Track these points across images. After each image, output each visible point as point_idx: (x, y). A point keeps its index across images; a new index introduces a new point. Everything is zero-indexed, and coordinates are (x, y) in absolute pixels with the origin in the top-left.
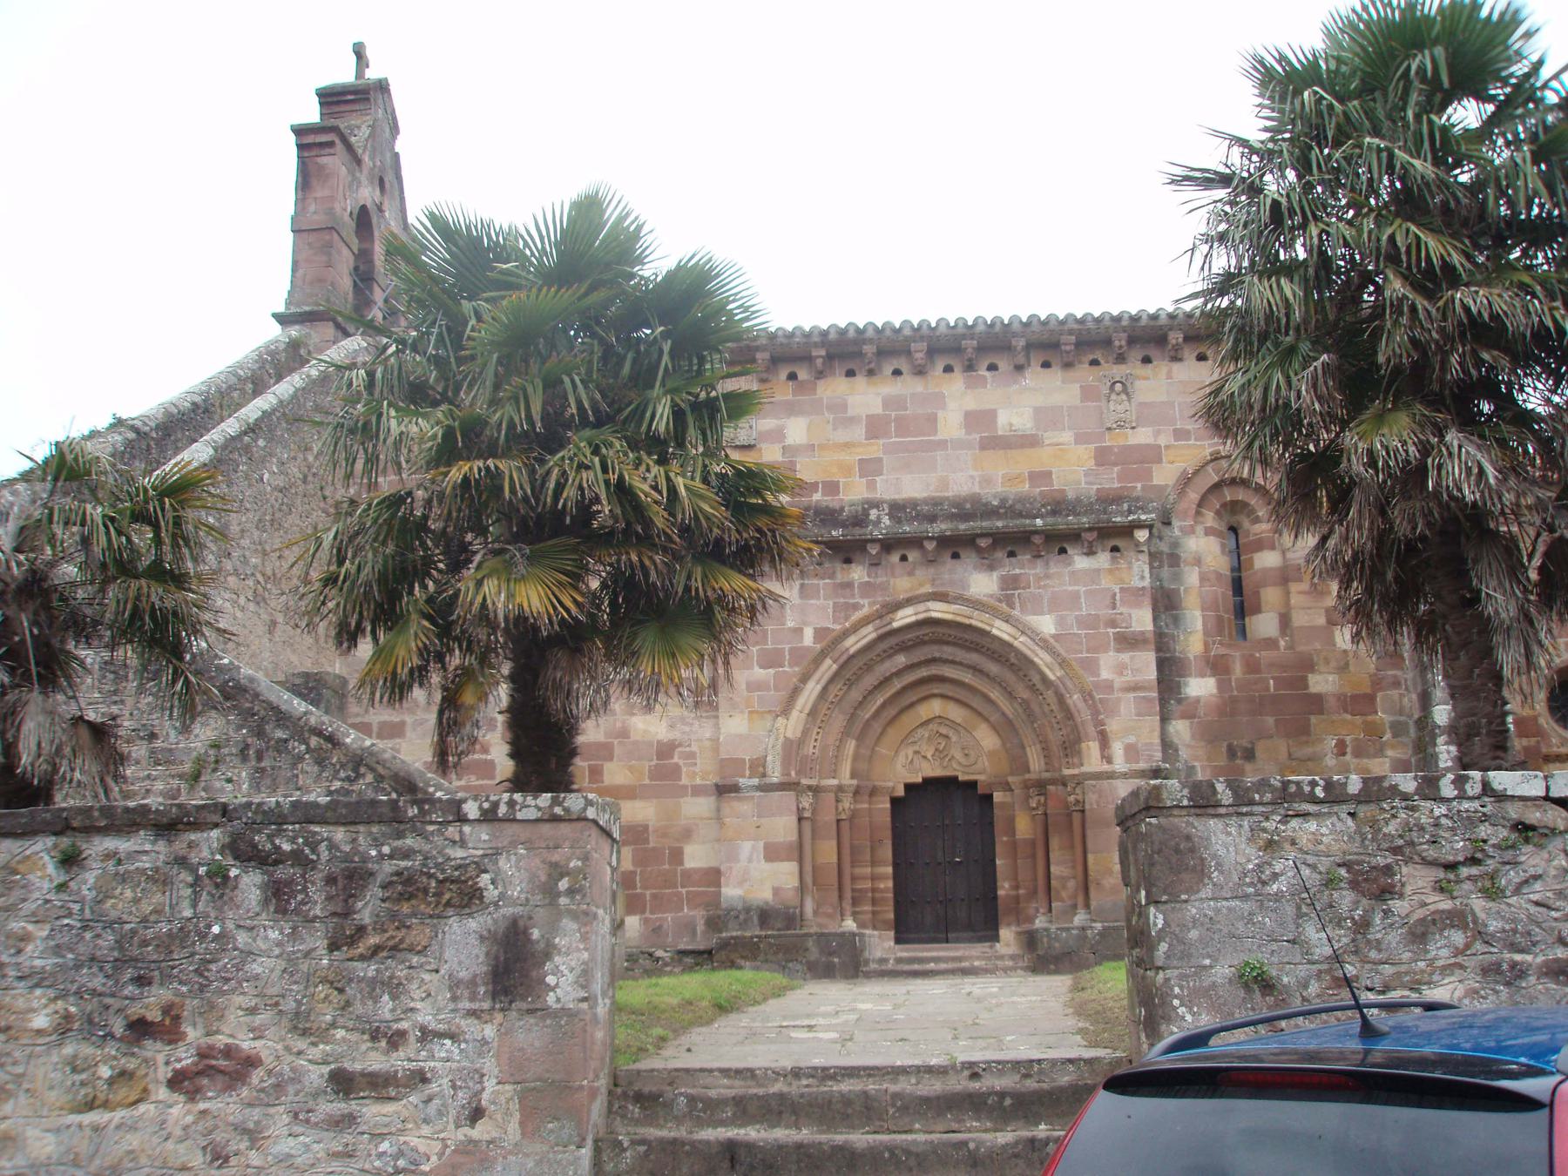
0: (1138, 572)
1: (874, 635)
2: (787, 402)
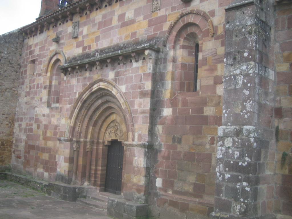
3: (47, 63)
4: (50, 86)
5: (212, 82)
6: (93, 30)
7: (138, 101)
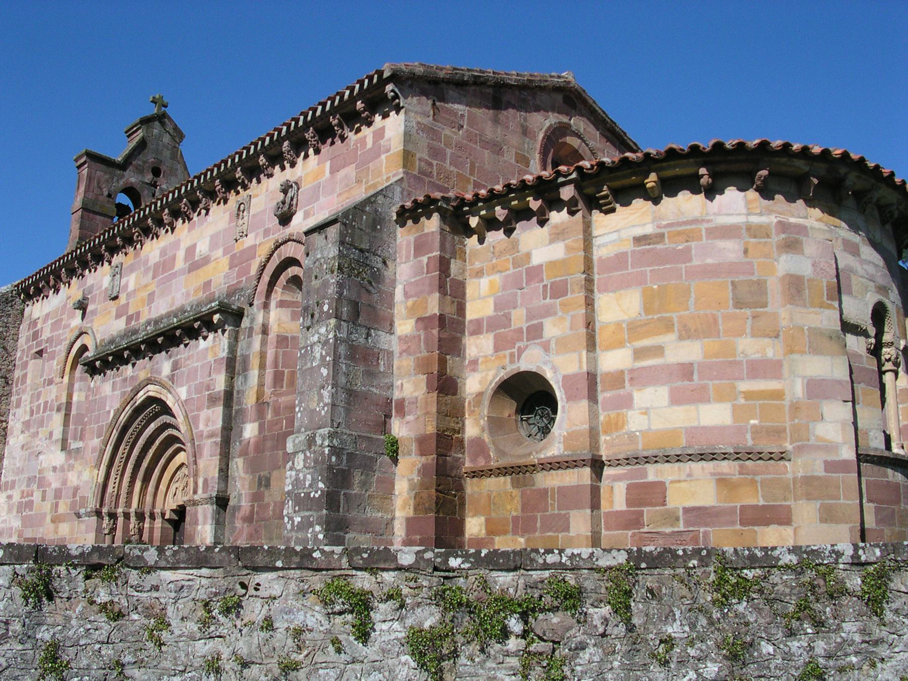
2: (132, 265)
3: (64, 354)
4: (69, 404)
6: (144, 281)
7: (204, 414)
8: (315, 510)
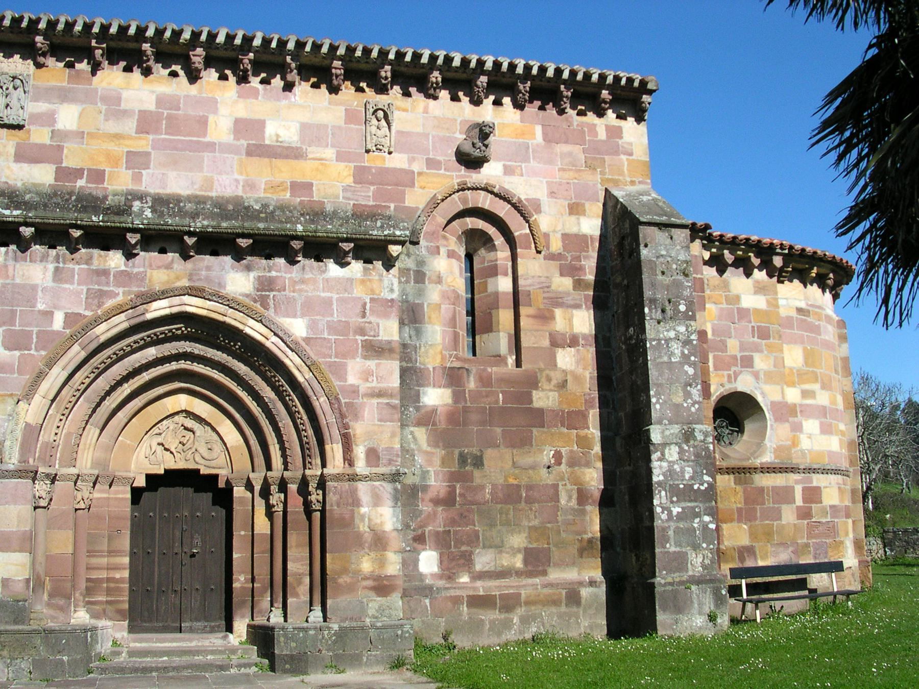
0: (387, 283)
1: (125, 325)
2: (61, 89)
5: (546, 343)
8: (701, 502)
